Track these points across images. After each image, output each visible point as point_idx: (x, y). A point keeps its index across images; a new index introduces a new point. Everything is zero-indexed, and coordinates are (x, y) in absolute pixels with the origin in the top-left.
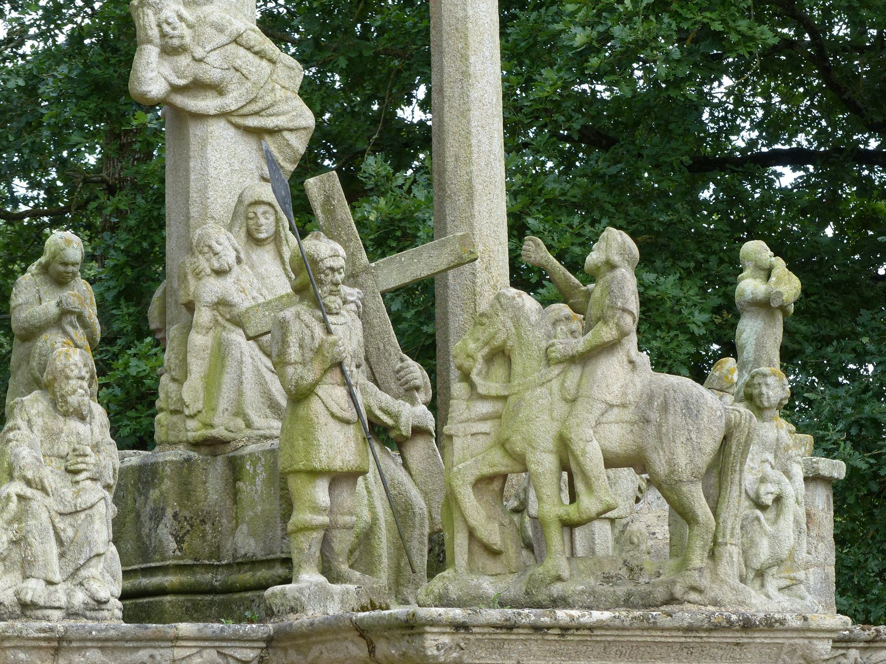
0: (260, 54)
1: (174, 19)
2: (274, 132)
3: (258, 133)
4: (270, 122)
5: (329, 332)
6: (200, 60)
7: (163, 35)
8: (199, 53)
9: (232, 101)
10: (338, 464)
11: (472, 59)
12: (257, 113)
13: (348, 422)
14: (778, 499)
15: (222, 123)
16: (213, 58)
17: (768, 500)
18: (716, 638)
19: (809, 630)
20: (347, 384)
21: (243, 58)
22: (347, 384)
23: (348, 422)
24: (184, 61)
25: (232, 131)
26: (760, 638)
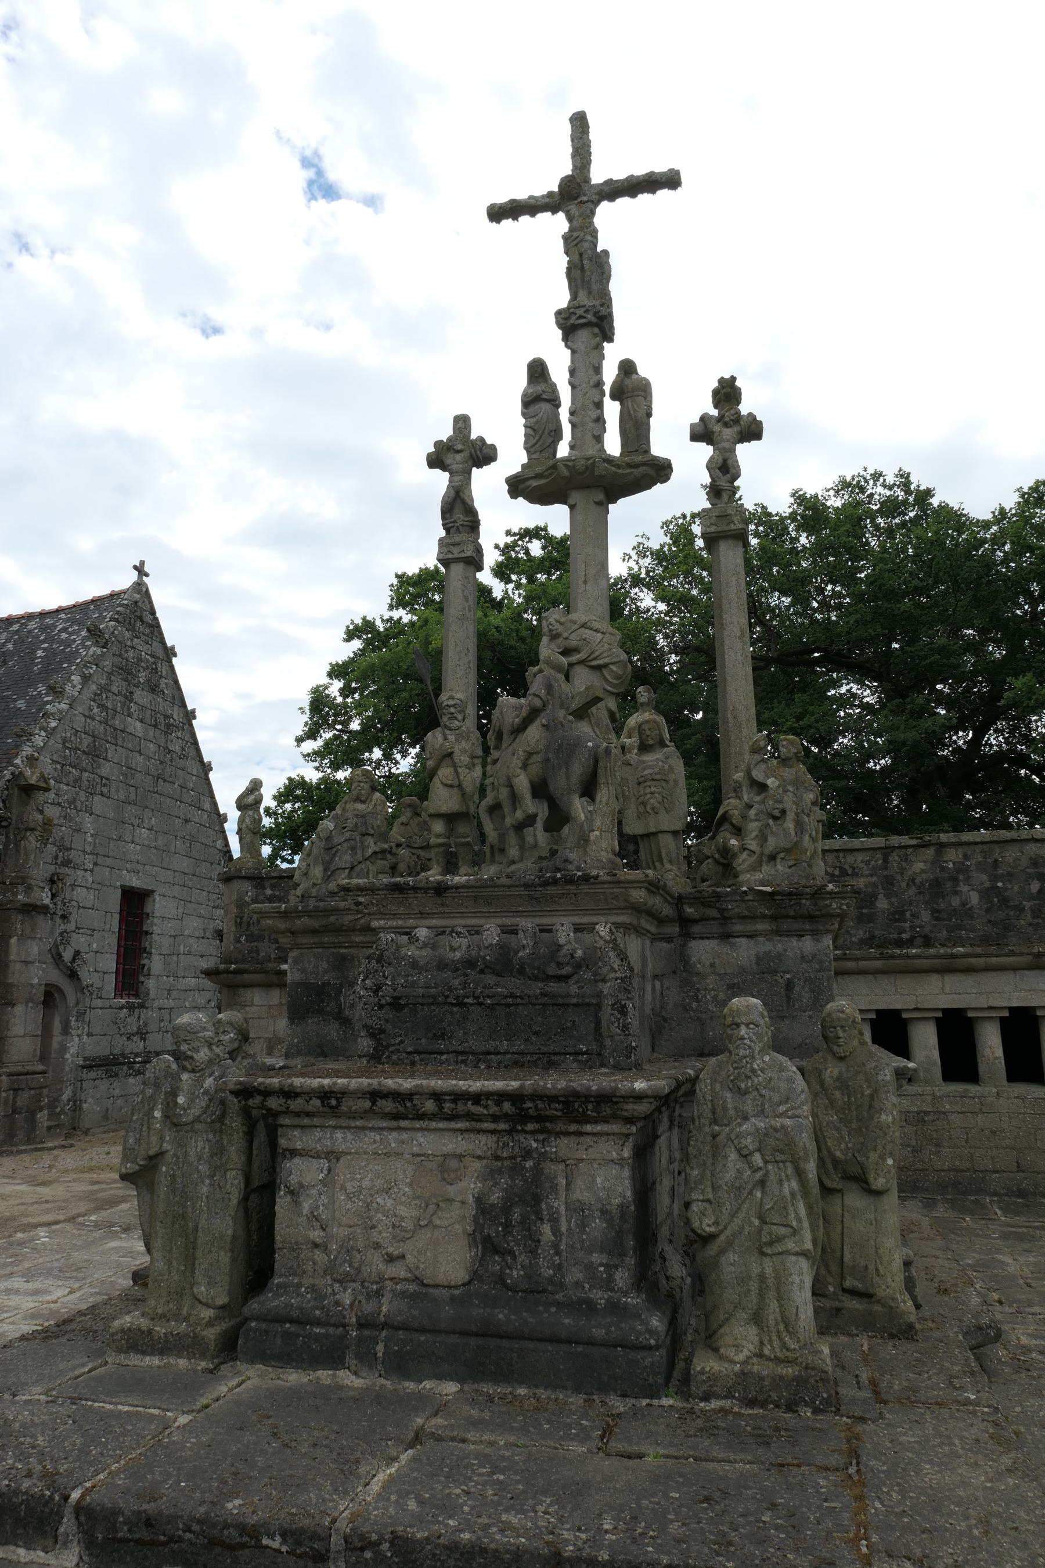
0: (597, 631)
1: (553, 622)
2: (605, 666)
3: (599, 668)
4: (601, 662)
5: (445, 739)
6: (566, 639)
7: (550, 630)
8: (565, 635)
9: (582, 656)
10: (444, 809)
11: (724, 616)
12: (595, 659)
13: (451, 786)
14: (783, 812)
15: (582, 666)
16: (573, 636)
17: (777, 813)
18: (552, 890)
19: (619, 882)
20: (455, 766)
21: (587, 633)
22: (455, 766)
23: (451, 786)
24: (561, 639)
25: (587, 670)
26: (585, 888)
